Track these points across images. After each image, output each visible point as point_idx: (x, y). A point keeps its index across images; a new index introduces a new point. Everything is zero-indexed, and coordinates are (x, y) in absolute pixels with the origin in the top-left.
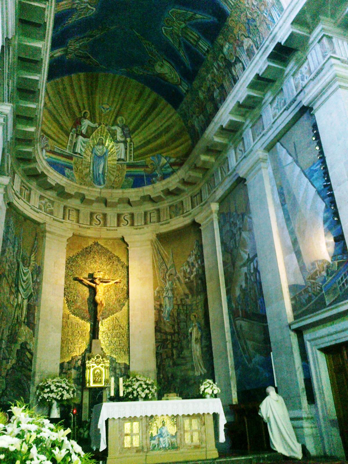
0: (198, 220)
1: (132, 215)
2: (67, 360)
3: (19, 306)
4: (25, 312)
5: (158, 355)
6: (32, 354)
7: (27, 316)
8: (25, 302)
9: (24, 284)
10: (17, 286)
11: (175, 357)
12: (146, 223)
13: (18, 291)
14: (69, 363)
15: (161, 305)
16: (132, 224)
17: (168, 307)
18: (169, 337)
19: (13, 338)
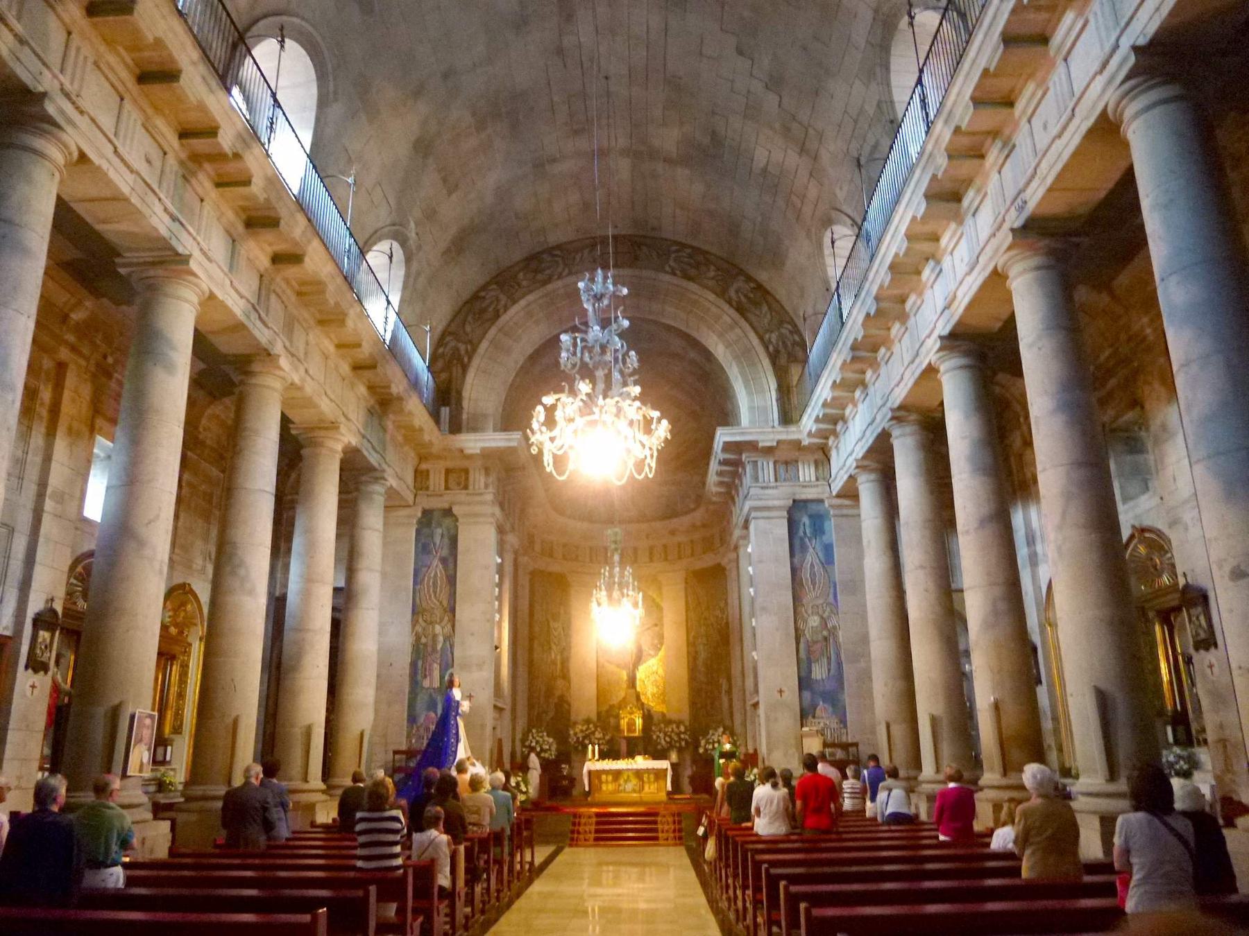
0: (724, 562)
1: (665, 546)
2: (605, 708)
3: (554, 663)
4: (559, 666)
5: (693, 704)
6: (569, 705)
7: (562, 670)
8: (559, 657)
9: (556, 641)
10: (549, 643)
11: (709, 708)
12: (680, 558)
13: (550, 648)
14: (607, 711)
15: (696, 652)
16: (666, 559)
17: (703, 656)
18: (704, 686)
19: (549, 692)
